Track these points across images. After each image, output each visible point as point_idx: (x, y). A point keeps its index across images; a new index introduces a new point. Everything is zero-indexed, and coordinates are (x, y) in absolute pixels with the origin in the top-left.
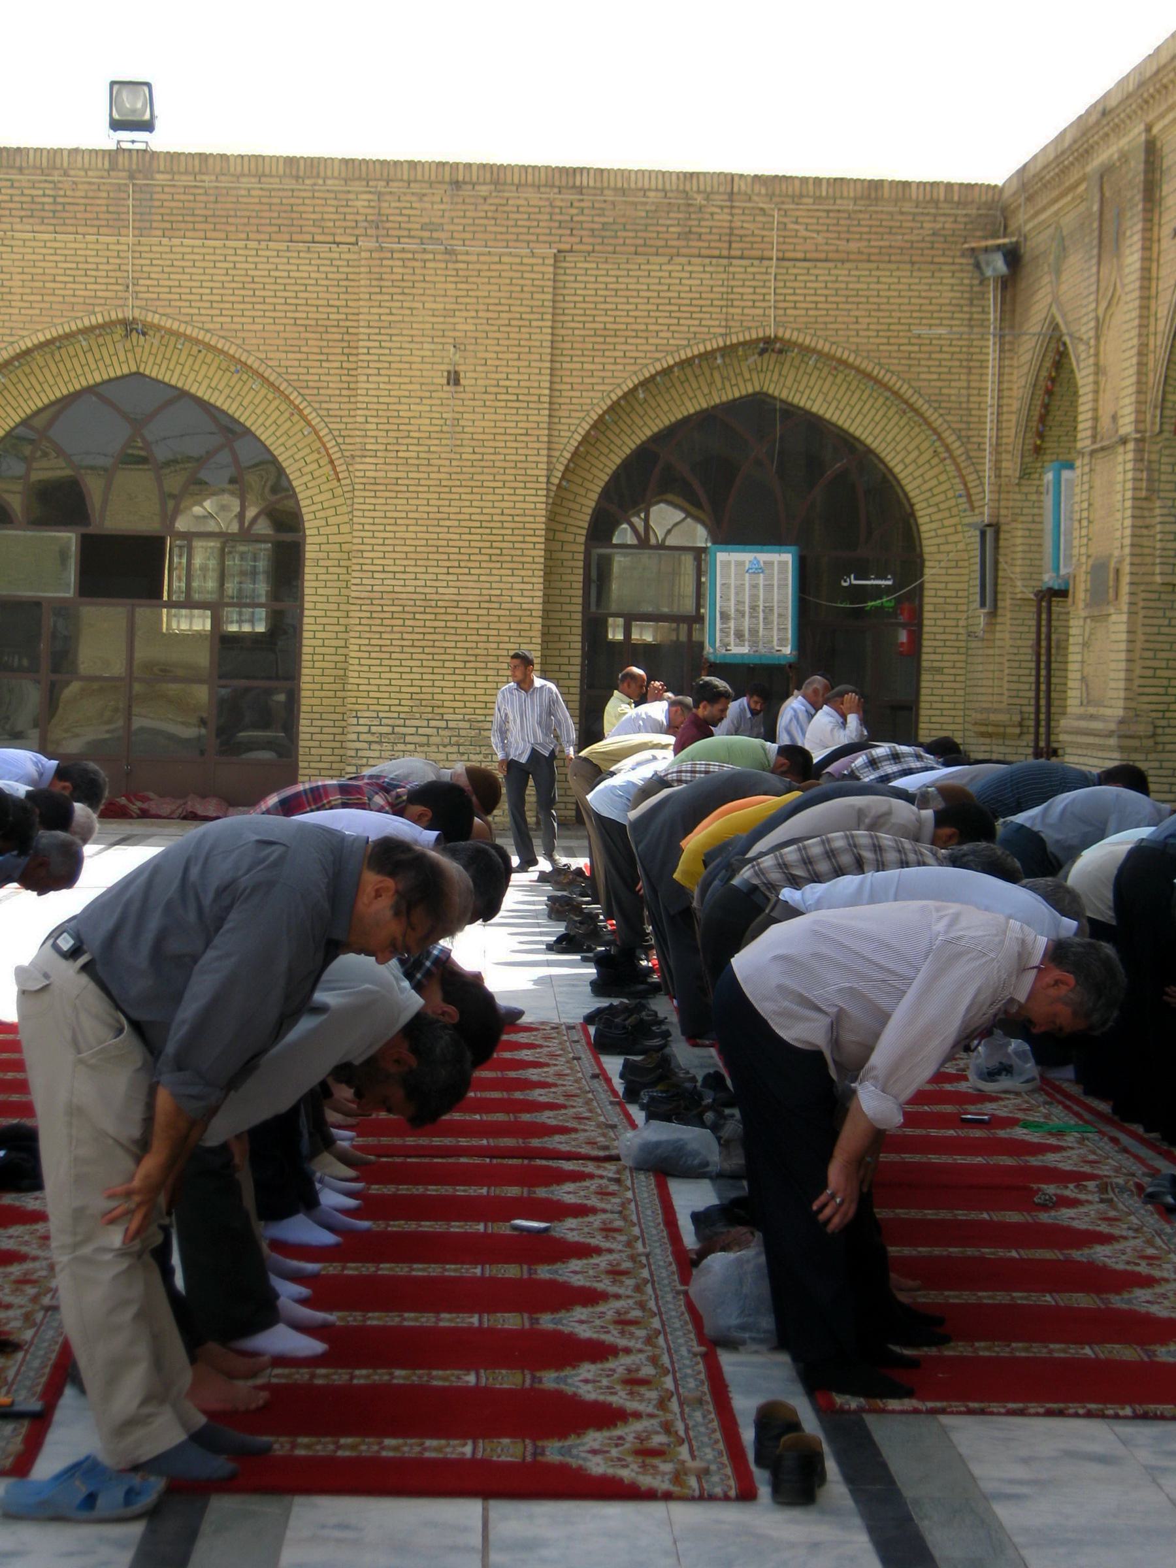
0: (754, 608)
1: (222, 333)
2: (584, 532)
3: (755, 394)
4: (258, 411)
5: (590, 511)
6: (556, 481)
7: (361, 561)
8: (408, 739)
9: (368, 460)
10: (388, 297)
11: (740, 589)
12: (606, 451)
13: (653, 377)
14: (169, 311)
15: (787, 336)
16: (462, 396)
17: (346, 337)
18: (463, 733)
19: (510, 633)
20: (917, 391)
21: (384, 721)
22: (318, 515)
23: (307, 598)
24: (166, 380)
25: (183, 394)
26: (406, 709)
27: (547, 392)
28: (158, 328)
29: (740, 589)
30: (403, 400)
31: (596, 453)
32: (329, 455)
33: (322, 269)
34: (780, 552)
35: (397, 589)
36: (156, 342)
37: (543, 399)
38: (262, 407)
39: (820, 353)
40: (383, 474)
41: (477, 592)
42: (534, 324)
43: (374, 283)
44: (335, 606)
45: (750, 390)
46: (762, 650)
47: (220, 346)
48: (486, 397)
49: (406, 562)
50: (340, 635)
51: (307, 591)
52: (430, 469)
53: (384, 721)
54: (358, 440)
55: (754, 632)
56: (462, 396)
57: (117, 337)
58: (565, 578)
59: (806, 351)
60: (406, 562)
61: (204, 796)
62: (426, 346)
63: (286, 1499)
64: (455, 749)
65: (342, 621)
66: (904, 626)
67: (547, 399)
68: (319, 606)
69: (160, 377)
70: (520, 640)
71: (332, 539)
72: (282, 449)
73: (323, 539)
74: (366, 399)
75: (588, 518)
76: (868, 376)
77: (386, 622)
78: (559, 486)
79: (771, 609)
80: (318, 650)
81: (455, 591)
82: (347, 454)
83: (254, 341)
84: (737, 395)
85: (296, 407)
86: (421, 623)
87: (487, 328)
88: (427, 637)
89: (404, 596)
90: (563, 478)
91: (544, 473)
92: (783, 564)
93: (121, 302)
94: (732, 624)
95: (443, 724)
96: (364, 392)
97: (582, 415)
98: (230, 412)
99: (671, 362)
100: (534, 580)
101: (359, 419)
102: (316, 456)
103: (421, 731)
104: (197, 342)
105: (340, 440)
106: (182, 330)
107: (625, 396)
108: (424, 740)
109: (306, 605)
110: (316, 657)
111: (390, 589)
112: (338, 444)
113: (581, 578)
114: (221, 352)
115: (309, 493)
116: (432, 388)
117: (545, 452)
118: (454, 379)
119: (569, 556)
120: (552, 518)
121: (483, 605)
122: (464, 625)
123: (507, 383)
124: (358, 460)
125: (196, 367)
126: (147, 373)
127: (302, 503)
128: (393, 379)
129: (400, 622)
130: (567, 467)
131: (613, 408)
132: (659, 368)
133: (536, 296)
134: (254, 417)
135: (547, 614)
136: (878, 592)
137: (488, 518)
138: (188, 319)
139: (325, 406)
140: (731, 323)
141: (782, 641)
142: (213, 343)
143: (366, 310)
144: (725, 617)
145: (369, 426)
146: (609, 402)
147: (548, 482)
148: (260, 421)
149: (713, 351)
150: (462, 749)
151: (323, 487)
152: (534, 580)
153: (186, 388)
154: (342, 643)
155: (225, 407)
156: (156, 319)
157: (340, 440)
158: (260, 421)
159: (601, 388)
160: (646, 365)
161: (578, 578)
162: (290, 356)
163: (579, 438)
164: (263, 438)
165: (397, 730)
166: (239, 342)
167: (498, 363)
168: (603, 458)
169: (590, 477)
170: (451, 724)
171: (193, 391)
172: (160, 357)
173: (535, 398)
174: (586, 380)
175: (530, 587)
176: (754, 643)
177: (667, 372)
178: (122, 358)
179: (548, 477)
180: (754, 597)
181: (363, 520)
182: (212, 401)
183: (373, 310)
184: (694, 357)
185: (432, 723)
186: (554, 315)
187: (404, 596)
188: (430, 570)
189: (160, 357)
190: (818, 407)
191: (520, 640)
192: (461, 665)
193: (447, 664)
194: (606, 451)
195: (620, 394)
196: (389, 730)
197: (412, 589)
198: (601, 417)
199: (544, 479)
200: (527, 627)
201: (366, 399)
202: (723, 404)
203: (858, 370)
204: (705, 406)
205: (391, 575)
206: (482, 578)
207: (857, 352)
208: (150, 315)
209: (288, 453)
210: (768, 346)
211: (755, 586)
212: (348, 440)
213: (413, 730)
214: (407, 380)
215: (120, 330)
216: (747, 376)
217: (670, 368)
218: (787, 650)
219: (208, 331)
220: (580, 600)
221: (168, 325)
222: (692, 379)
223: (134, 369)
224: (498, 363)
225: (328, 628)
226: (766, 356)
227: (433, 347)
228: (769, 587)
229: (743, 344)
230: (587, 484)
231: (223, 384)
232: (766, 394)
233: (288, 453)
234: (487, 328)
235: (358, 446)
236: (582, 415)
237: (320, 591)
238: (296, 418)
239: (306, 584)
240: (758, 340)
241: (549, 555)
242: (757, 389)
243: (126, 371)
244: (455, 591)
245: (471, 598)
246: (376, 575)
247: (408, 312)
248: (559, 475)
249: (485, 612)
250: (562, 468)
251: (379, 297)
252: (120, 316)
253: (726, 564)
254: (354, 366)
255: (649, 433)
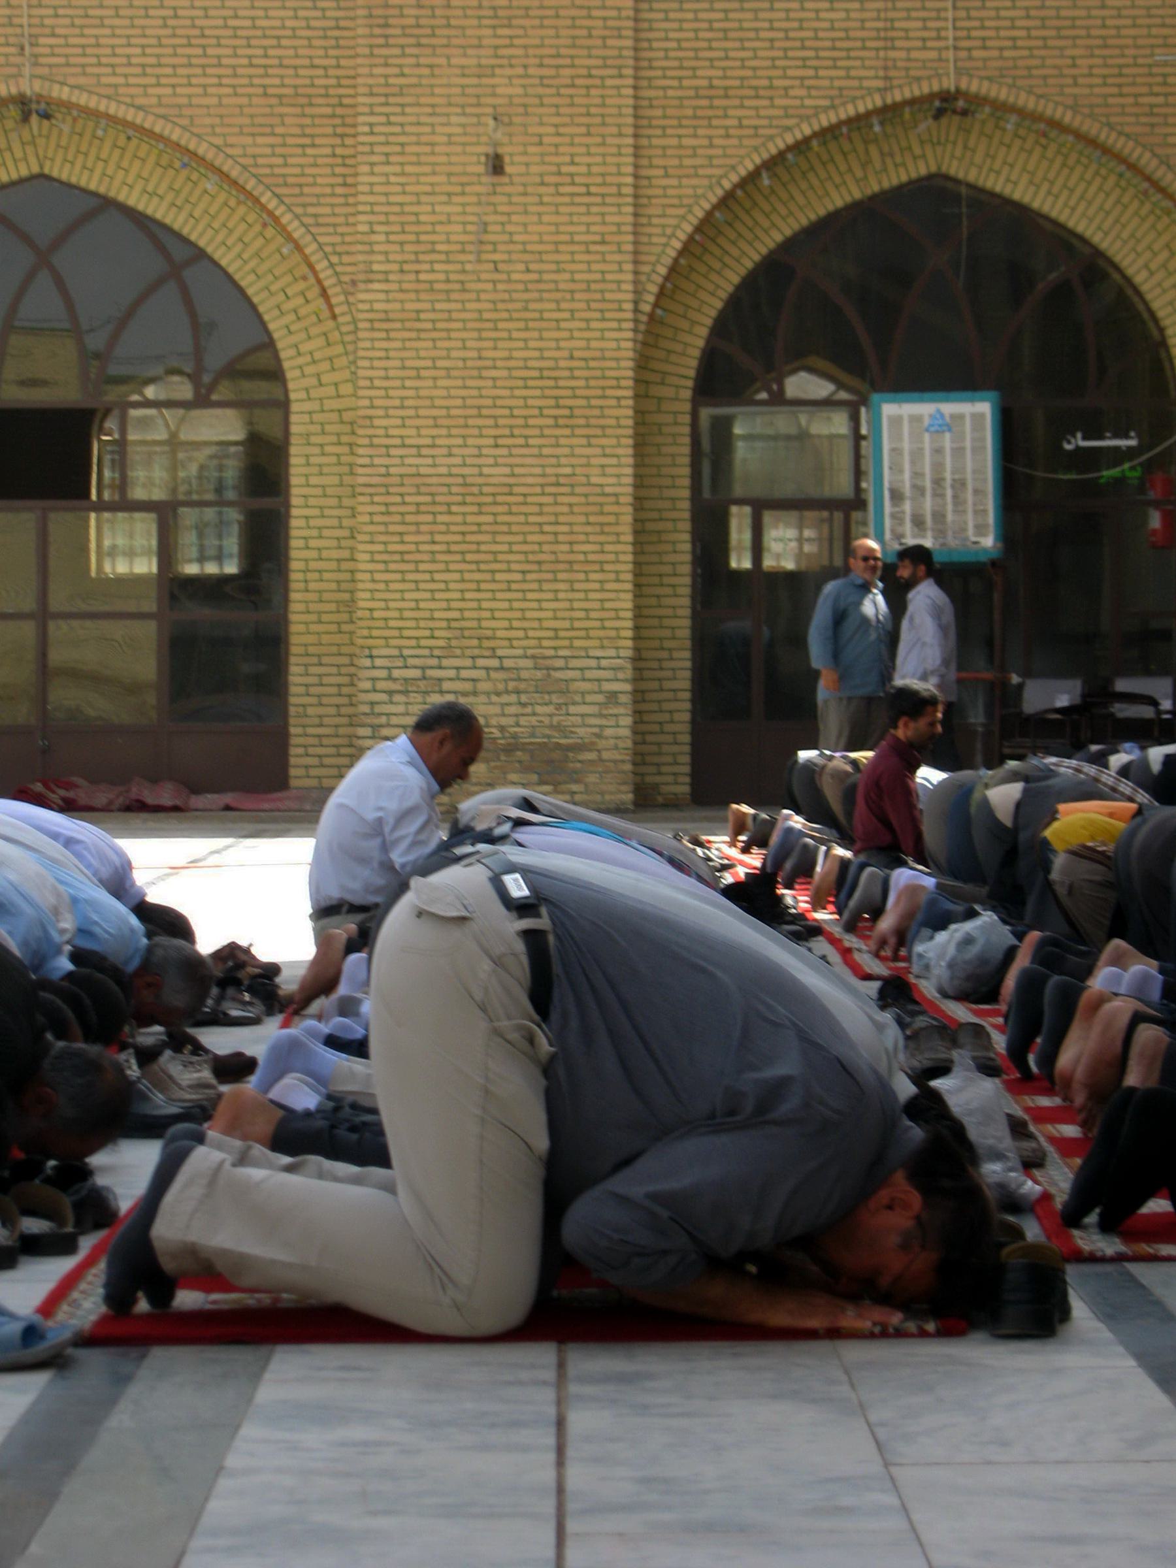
0: (938, 482)
1: (162, 111)
2: (690, 383)
3: (930, 177)
4: (216, 225)
5: (697, 353)
6: (647, 308)
7: (370, 432)
8: (446, 686)
9: (376, 286)
10: (397, 51)
11: (917, 455)
12: (717, 265)
13: (781, 155)
14: (82, 81)
15: (974, 88)
16: (508, 189)
17: (339, 111)
18: (525, 674)
19: (589, 529)
20: (1165, 162)
21: (411, 661)
22: (309, 370)
23: (294, 491)
24: (83, 183)
25: (106, 204)
26: (441, 643)
27: (630, 180)
28: (68, 105)
29: (917, 455)
30: (424, 199)
31: (703, 269)
32: (319, 281)
33: (301, 13)
34: (972, 401)
35: (423, 471)
36: (66, 129)
37: (625, 190)
38: (222, 217)
39: (1021, 112)
40: (398, 306)
41: (538, 471)
42: (609, 82)
43: (377, 31)
44: (333, 502)
45: (923, 171)
46: (952, 542)
47: (157, 129)
48: (543, 190)
49: (435, 432)
50: (343, 543)
51: (294, 481)
52: (467, 296)
53: (411, 661)
54: (361, 258)
55: (939, 516)
56: (508, 189)
57: (10, 124)
58: (664, 450)
59: (1001, 108)
60: (435, 432)
61: (155, 780)
62: (454, 119)
63: (264, 1349)
64: (513, 698)
65: (346, 523)
66: (1156, 504)
67: (628, 190)
68: (312, 501)
69: (74, 180)
70: (602, 538)
71: (329, 404)
72: (252, 277)
73: (315, 406)
74: (371, 199)
75: (694, 363)
76: (1092, 142)
77: (409, 518)
78: (651, 316)
79: (963, 484)
80: (313, 565)
81: (507, 470)
82: (346, 279)
83: (208, 121)
84: (904, 178)
85: (270, 214)
86: (459, 519)
87: (541, 91)
88: (469, 538)
89: (434, 480)
90: (656, 305)
91: (630, 296)
92: (978, 418)
93: (14, 71)
94: (907, 507)
95: (495, 663)
96: (366, 189)
97: (681, 212)
98: (176, 227)
99: (807, 131)
100: (620, 451)
101: (361, 228)
102: (302, 285)
103: (464, 674)
104: (125, 123)
105: (335, 259)
106: (102, 108)
107: (743, 183)
108: (468, 686)
109: (294, 501)
110: (310, 576)
111: (413, 470)
112: (332, 265)
113: (686, 450)
114: (160, 138)
115: (294, 339)
116: (464, 179)
117: (629, 267)
118: (497, 166)
119: (669, 419)
120: (643, 364)
121: (548, 490)
122: (522, 519)
123: (572, 169)
124: (362, 286)
125: (125, 164)
126: (55, 174)
127: (283, 355)
128: (409, 169)
129: (429, 518)
130: (662, 288)
131: (727, 201)
132: (790, 140)
133: (610, 42)
134: (210, 232)
135: (639, 503)
136: (1117, 456)
137: (551, 364)
138: (110, 91)
139: (311, 210)
140: (892, 73)
141: (980, 529)
142: (147, 125)
143: (365, 71)
144: (897, 496)
145: (375, 238)
146: (720, 193)
147: (636, 310)
148: (220, 237)
149: (868, 114)
150: (524, 698)
151: (314, 331)
152: (620, 451)
153: (112, 194)
154: (346, 554)
155: (168, 221)
156: (65, 93)
157: (335, 259)
158: (220, 237)
159: (709, 171)
160: (771, 138)
161: (683, 450)
162: (260, 140)
163: (678, 245)
164: (223, 263)
165: (429, 673)
166: (185, 122)
167: (557, 140)
168: (714, 277)
169: (695, 304)
170: (508, 663)
171: (121, 198)
172: (73, 149)
173: (614, 190)
174: (687, 162)
175: (614, 461)
176: (940, 533)
177: (802, 146)
178: (19, 154)
179: (636, 303)
180: (938, 467)
181: (370, 373)
182: (149, 212)
183: (376, 71)
184: (841, 123)
185: (481, 662)
186: (636, 68)
187: (434, 480)
188: (470, 441)
189: (73, 149)
190: (1020, 193)
191: (602, 538)
192: (519, 577)
193: (498, 576)
194: (717, 265)
195: (735, 178)
196: (417, 673)
197: (443, 470)
198: (709, 214)
199: (629, 306)
200: (612, 519)
201: (371, 199)
202: (883, 193)
203: (1078, 135)
204: (857, 195)
205: (414, 451)
206: (545, 451)
207: (1075, 108)
208: (56, 87)
209: (261, 284)
210: (947, 105)
211: (938, 451)
212: (346, 259)
213: (452, 673)
214: (427, 169)
215: (14, 112)
216: (917, 151)
217: (806, 140)
218: (988, 541)
219: (139, 108)
220: (687, 482)
221: (82, 102)
222: (838, 158)
223: (36, 169)
224: (557, 140)
225: (326, 533)
226: (944, 121)
227: (463, 120)
228: (958, 452)
229: (912, 102)
230: (692, 314)
231: (164, 187)
232: (947, 177)
233: (261, 284)
234: (541, 91)
235: (361, 267)
236: (681, 212)
237: (314, 480)
238: (270, 232)
239: (293, 471)
240: (932, 96)
241: (641, 417)
242: (933, 169)
243: (24, 172)
244: (507, 470)
245: (530, 480)
246: (393, 452)
247: (427, 71)
248: (651, 299)
249: (550, 500)
250: (654, 289)
251: (384, 51)
252: (14, 91)
253: (896, 421)
254: (350, 151)
255: (779, 238)
